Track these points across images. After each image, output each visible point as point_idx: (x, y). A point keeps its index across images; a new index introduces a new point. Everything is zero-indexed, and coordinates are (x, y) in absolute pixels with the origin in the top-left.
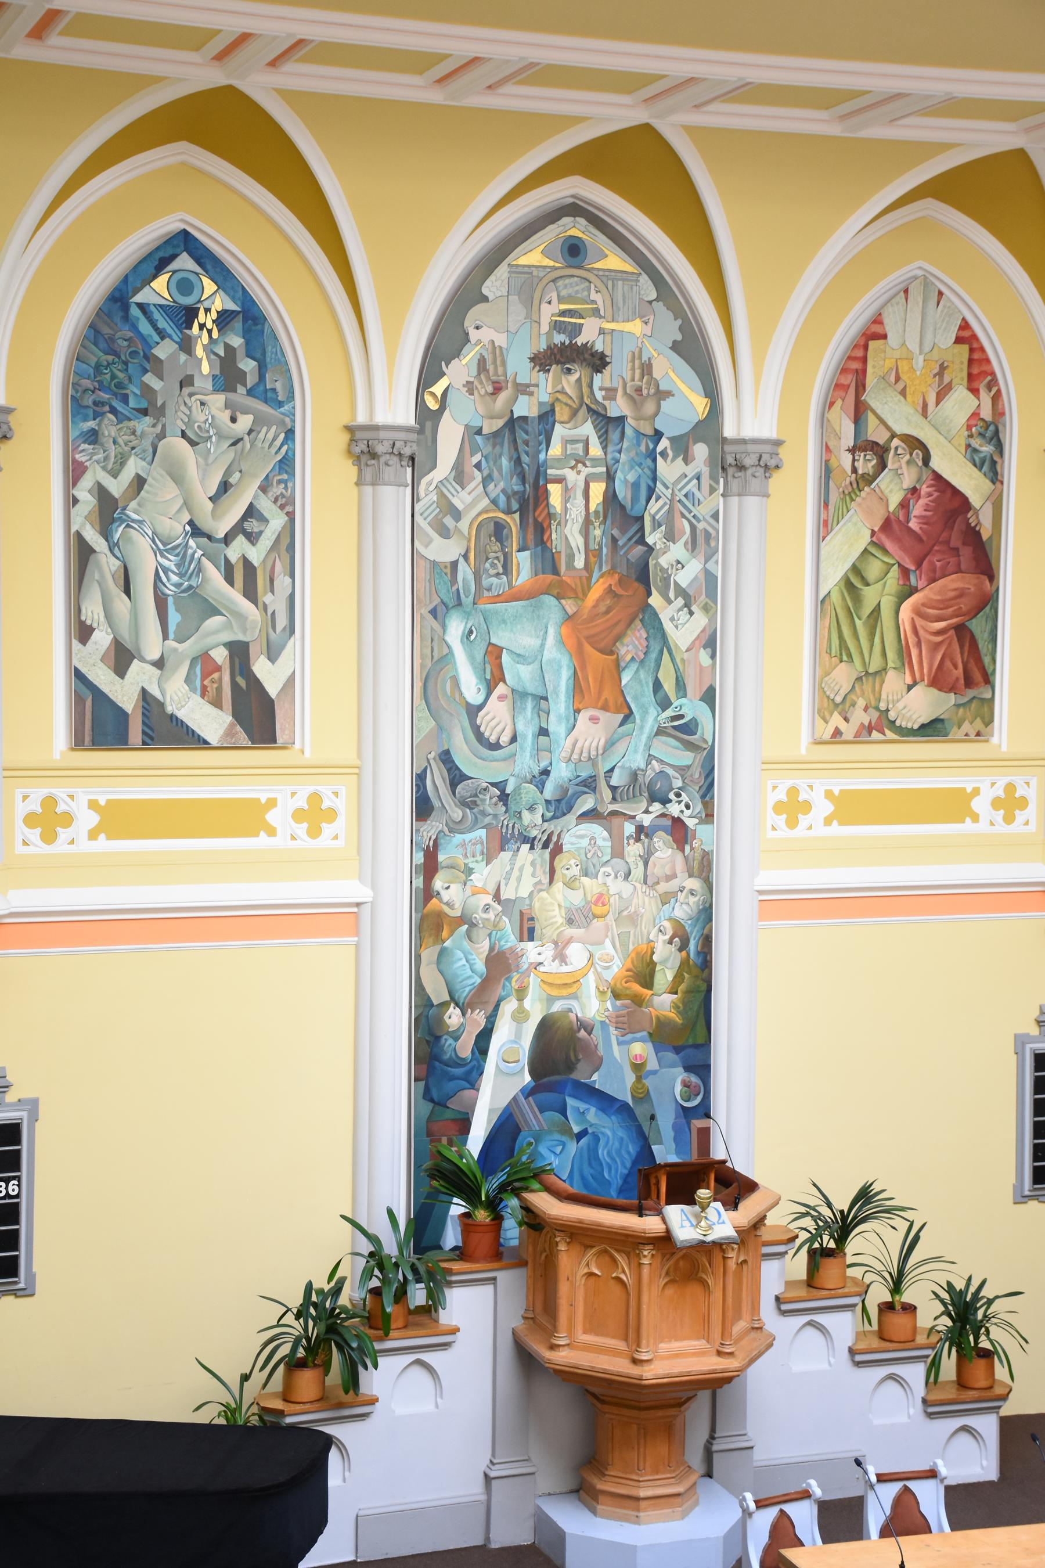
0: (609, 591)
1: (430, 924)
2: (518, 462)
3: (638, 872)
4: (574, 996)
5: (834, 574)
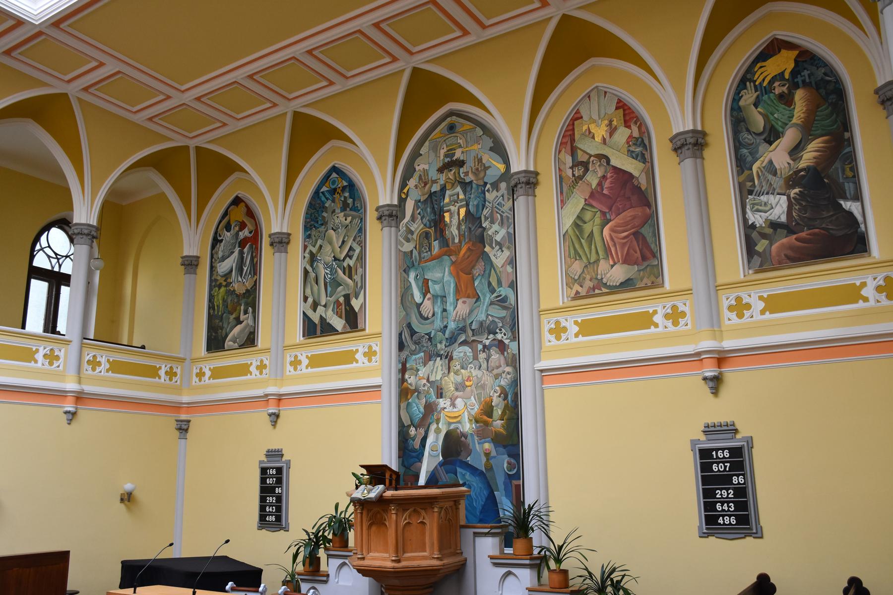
0: (469, 249)
1: (404, 393)
2: (433, 208)
3: (484, 365)
4: (459, 422)
5: (568, 222)
